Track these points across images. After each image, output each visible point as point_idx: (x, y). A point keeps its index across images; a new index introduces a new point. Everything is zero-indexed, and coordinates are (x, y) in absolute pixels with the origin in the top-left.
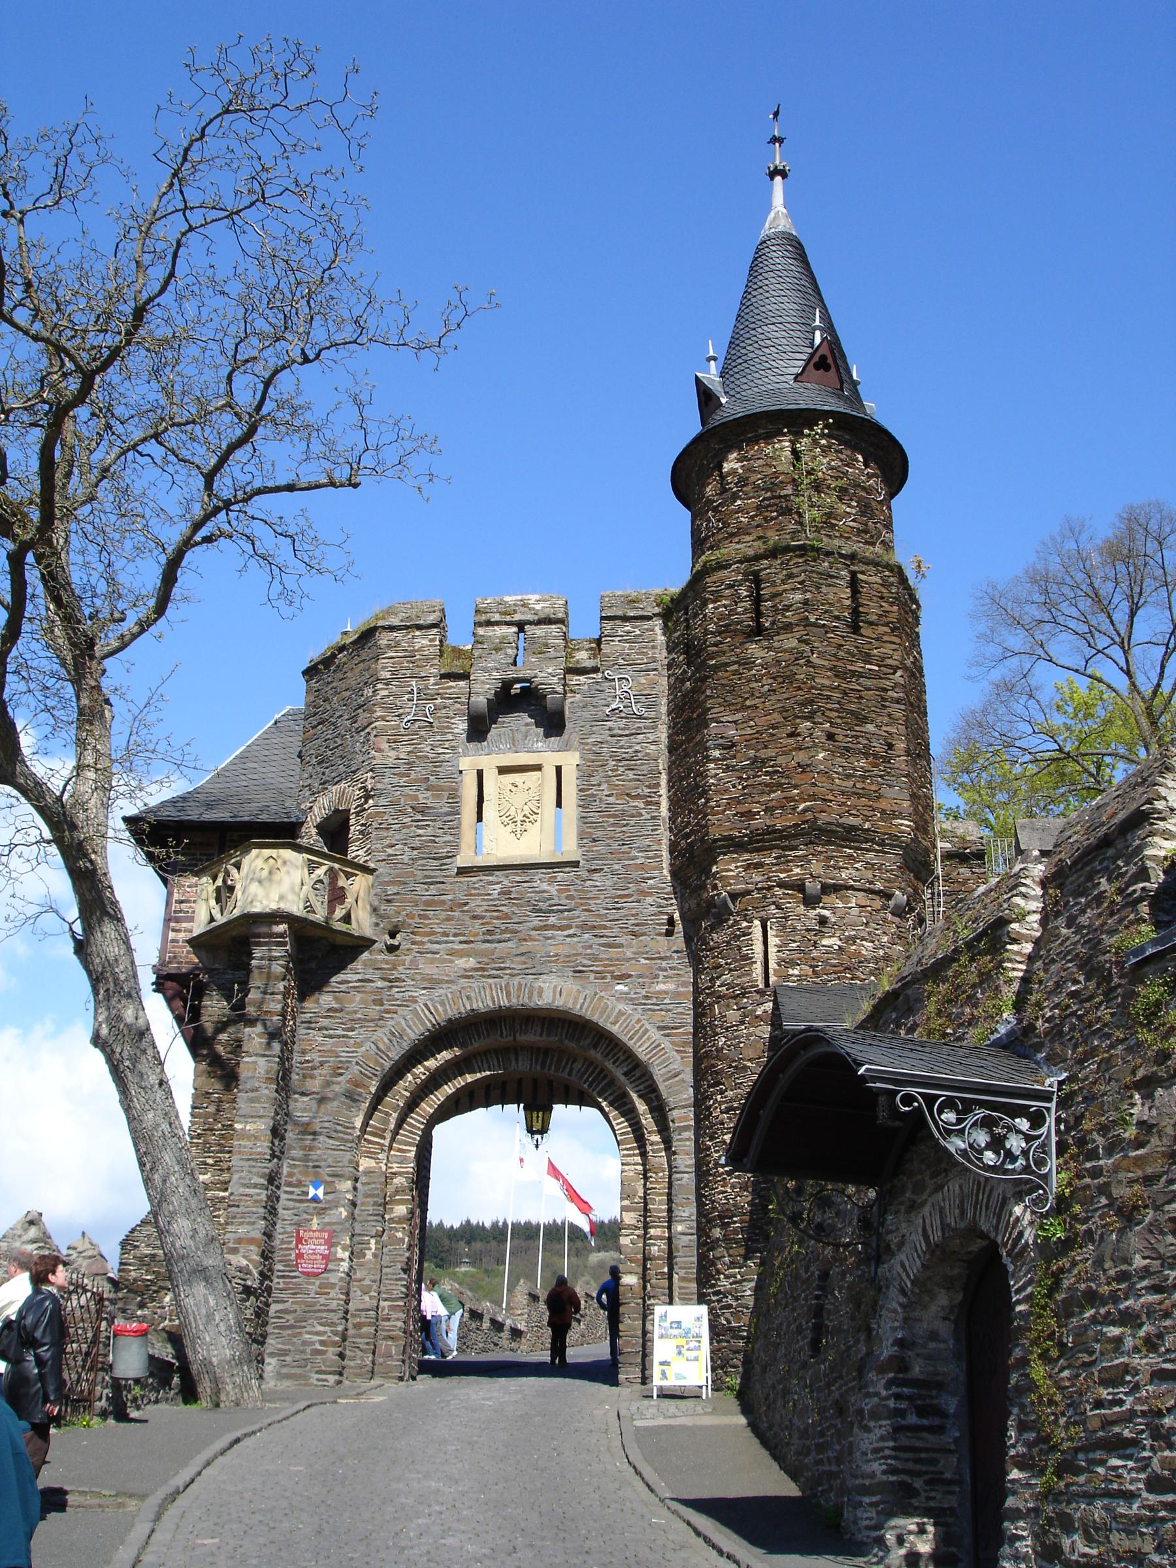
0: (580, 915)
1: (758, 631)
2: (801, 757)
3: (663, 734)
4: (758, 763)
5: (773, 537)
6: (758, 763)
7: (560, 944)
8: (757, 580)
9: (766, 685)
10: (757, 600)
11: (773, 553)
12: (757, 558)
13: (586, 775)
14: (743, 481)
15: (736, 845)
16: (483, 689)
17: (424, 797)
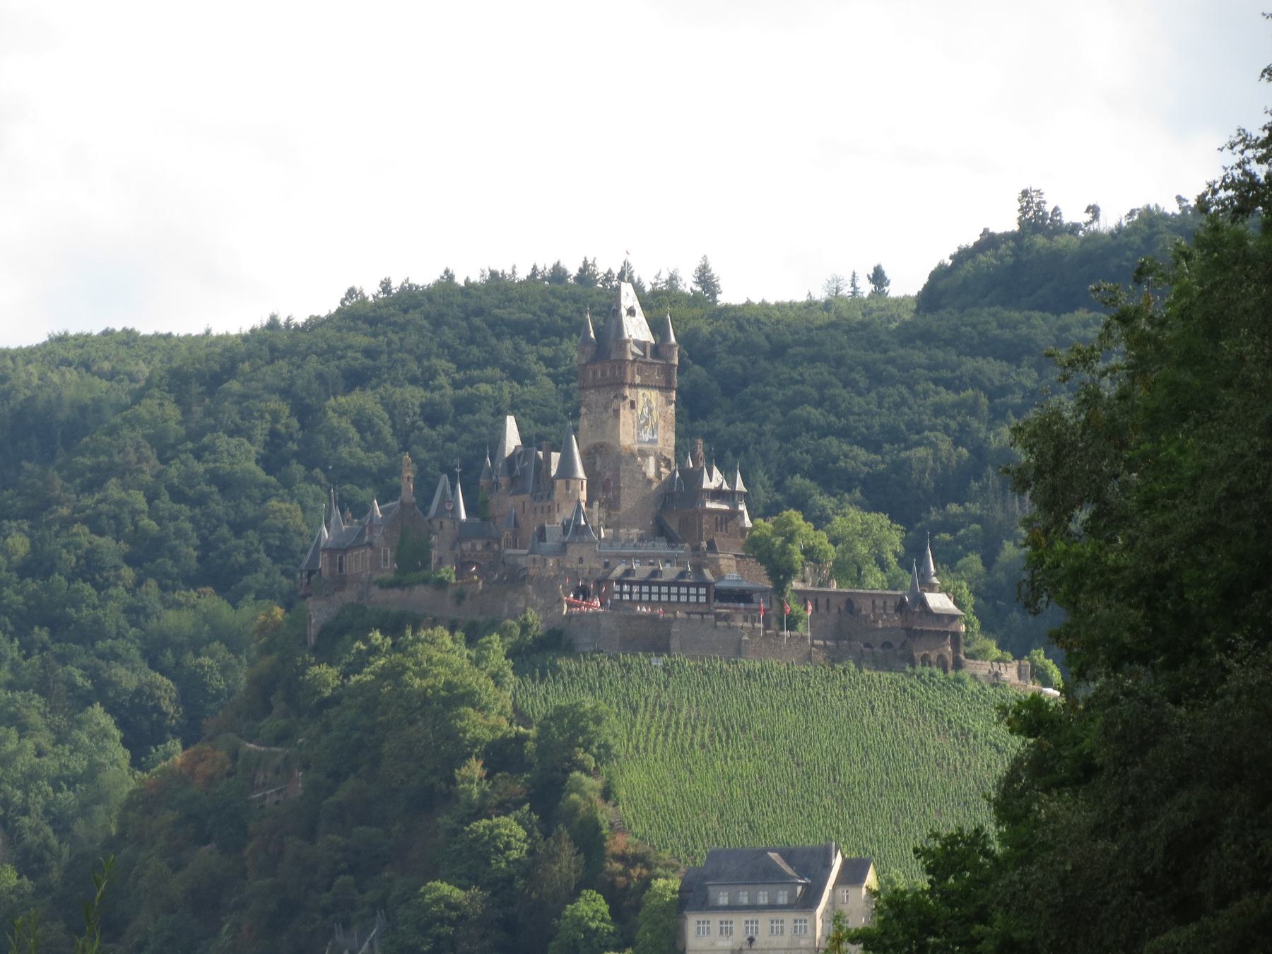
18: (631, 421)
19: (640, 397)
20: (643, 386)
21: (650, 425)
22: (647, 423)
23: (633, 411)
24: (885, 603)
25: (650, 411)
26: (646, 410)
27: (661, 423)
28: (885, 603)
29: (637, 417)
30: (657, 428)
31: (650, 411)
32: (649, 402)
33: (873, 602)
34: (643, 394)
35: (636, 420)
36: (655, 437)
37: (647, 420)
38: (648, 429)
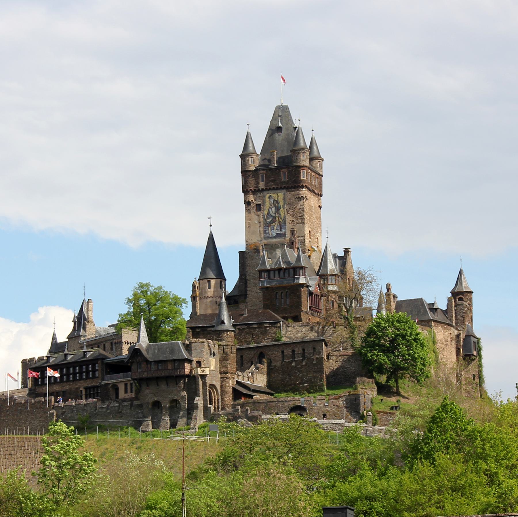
1: (232, 353)
18: (256, 222)
19: (267, 199)
20: (267, 189)
21: (277, 223)
22: (274, 221)
23: (259, 213)
24: (293, 351)
25: (278, 209)
26: (273, 209)
28: (293, 351)
29: (263, 217)
31: (278, 209)
32: (276, 202)
33: (283, 352)
34: (270, 197)
35: (262, 220)
36: (283, 231)
37: (275, 217)
38: (276, 226)
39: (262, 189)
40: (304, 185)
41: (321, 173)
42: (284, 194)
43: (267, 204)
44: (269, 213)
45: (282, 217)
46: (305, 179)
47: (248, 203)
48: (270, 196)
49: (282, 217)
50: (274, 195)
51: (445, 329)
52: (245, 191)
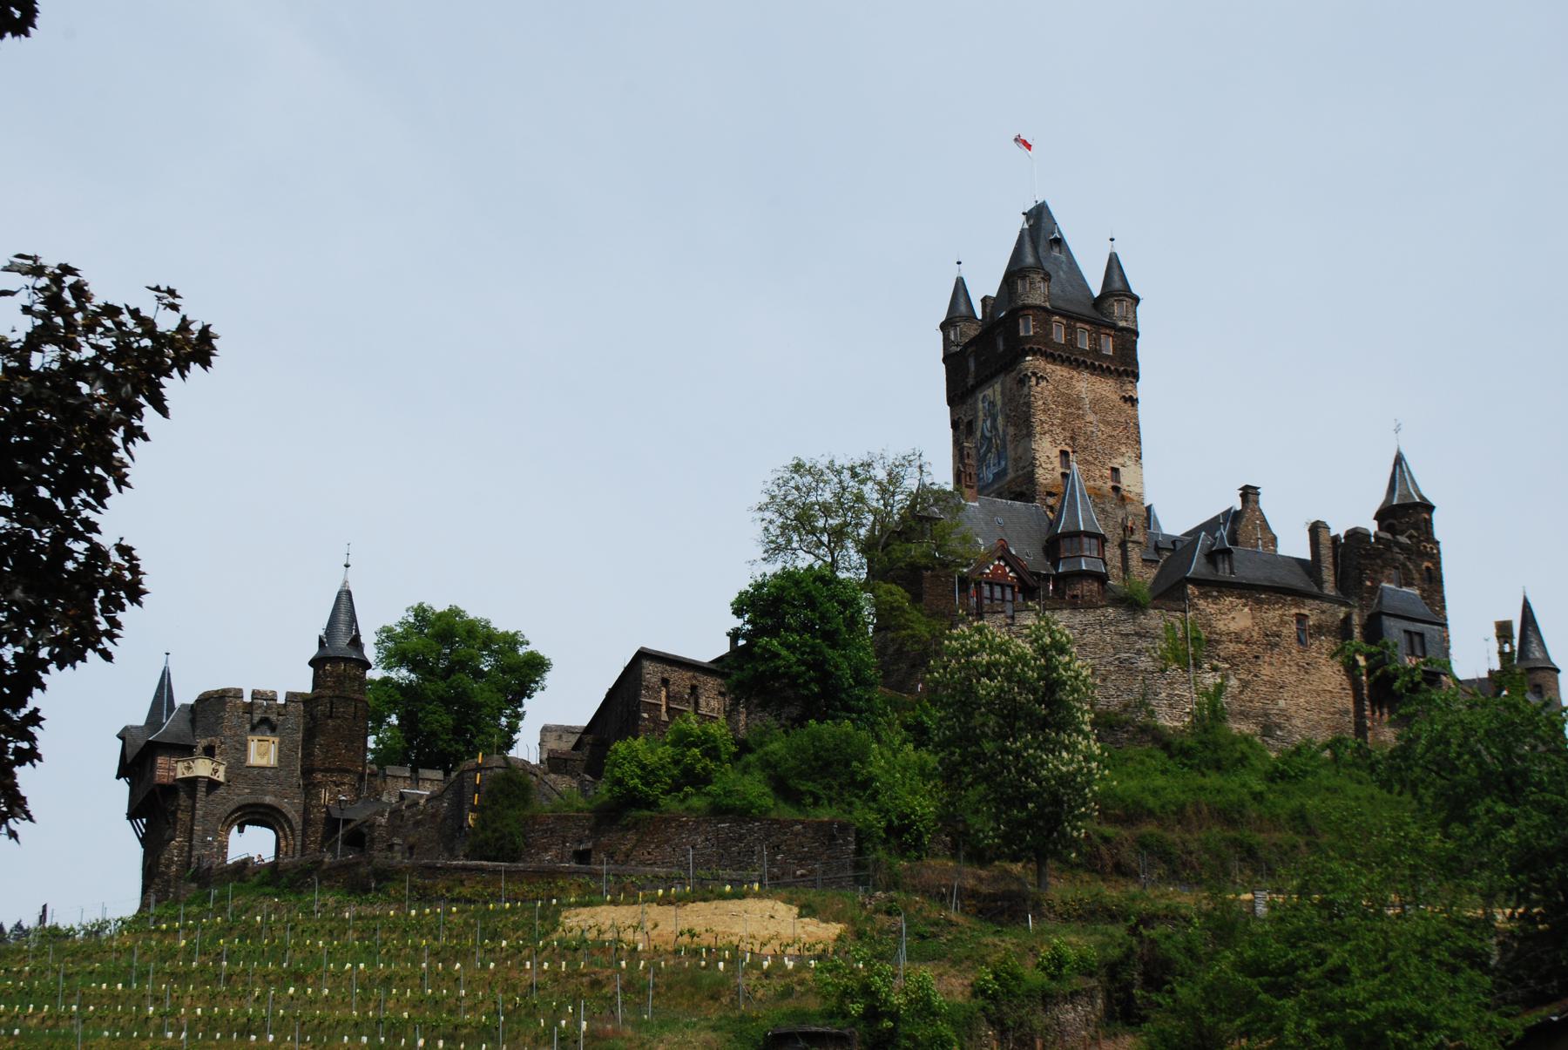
0: (277, 781)
1: (330, 717)
2: (338, 751)
3: (301, 735)
4: (328, 751)
5: (337, 692)
6: (328, 751)
7: (271, 788)
8: (332, 703)
9: (332, 732)
10: (332, 708)
11: (337, 697)
12: (333, 697)
13: (280, 744)
14: (331, 673)
15: (322, 771)
16: (256, 718)
17: (238, 746)
19: (980, 405)
26: (988, 423)
27: (1011, 430)
30: (1004, 446)
39: (972, 386)
40: (1027, 347)
41: (1122, 324)
42: (1002, 384)
43: (981, 414)
44: (983, 435)
45: (1001, 432)
46: (1032, 333)
47: (955, 425)
48: (984, 396)
49: (1001, 432)
50: (989, 392)
51: (1259, 602)
52: (950, 401)
